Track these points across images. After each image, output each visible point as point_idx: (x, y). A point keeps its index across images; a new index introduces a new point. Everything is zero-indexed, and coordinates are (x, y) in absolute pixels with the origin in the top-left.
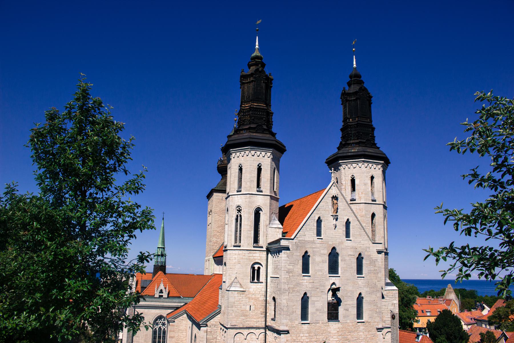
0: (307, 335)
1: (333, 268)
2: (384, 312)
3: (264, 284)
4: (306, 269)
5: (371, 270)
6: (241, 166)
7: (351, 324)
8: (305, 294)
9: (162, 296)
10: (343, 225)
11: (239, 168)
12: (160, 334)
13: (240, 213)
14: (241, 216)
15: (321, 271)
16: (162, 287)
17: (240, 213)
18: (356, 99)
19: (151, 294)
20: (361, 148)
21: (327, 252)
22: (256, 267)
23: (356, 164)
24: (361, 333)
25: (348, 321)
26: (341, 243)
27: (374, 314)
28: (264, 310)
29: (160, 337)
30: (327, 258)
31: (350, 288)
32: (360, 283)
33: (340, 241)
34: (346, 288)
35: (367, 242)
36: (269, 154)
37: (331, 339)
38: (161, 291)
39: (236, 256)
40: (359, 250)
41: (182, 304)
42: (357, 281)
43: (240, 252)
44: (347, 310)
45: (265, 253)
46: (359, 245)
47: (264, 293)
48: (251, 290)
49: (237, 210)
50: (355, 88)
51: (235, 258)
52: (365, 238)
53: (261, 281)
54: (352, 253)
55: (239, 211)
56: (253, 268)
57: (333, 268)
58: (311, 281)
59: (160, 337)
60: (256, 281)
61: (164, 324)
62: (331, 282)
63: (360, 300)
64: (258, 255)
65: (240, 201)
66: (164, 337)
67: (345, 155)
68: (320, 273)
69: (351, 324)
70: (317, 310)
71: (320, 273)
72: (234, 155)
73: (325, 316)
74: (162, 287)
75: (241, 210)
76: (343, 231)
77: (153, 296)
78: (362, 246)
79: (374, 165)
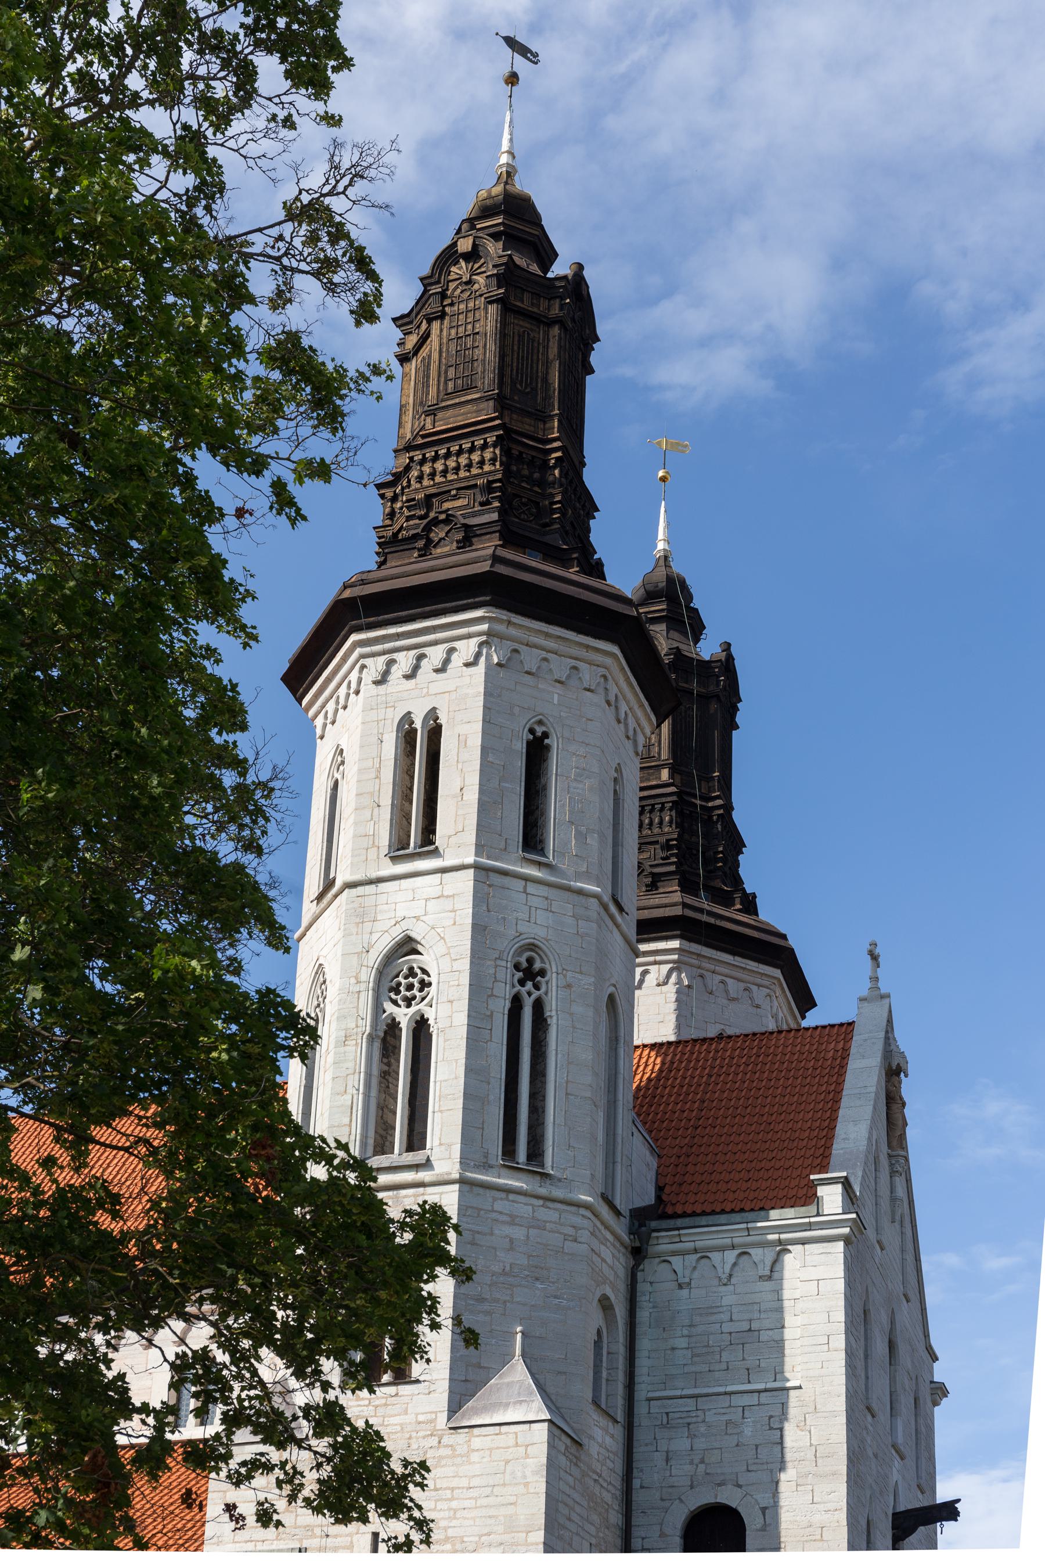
6: (539, 730)
11: (531, 737)
13: (537, 987)
14: (538, 1007)
17: (537, 987)
23: (742, 985)
39: (518, 1233)
43: (549, 1214)
49: (517, 967)
51: (511, 1241)
55: (530, 974)
65: (541, 917)
75: (542, 973)
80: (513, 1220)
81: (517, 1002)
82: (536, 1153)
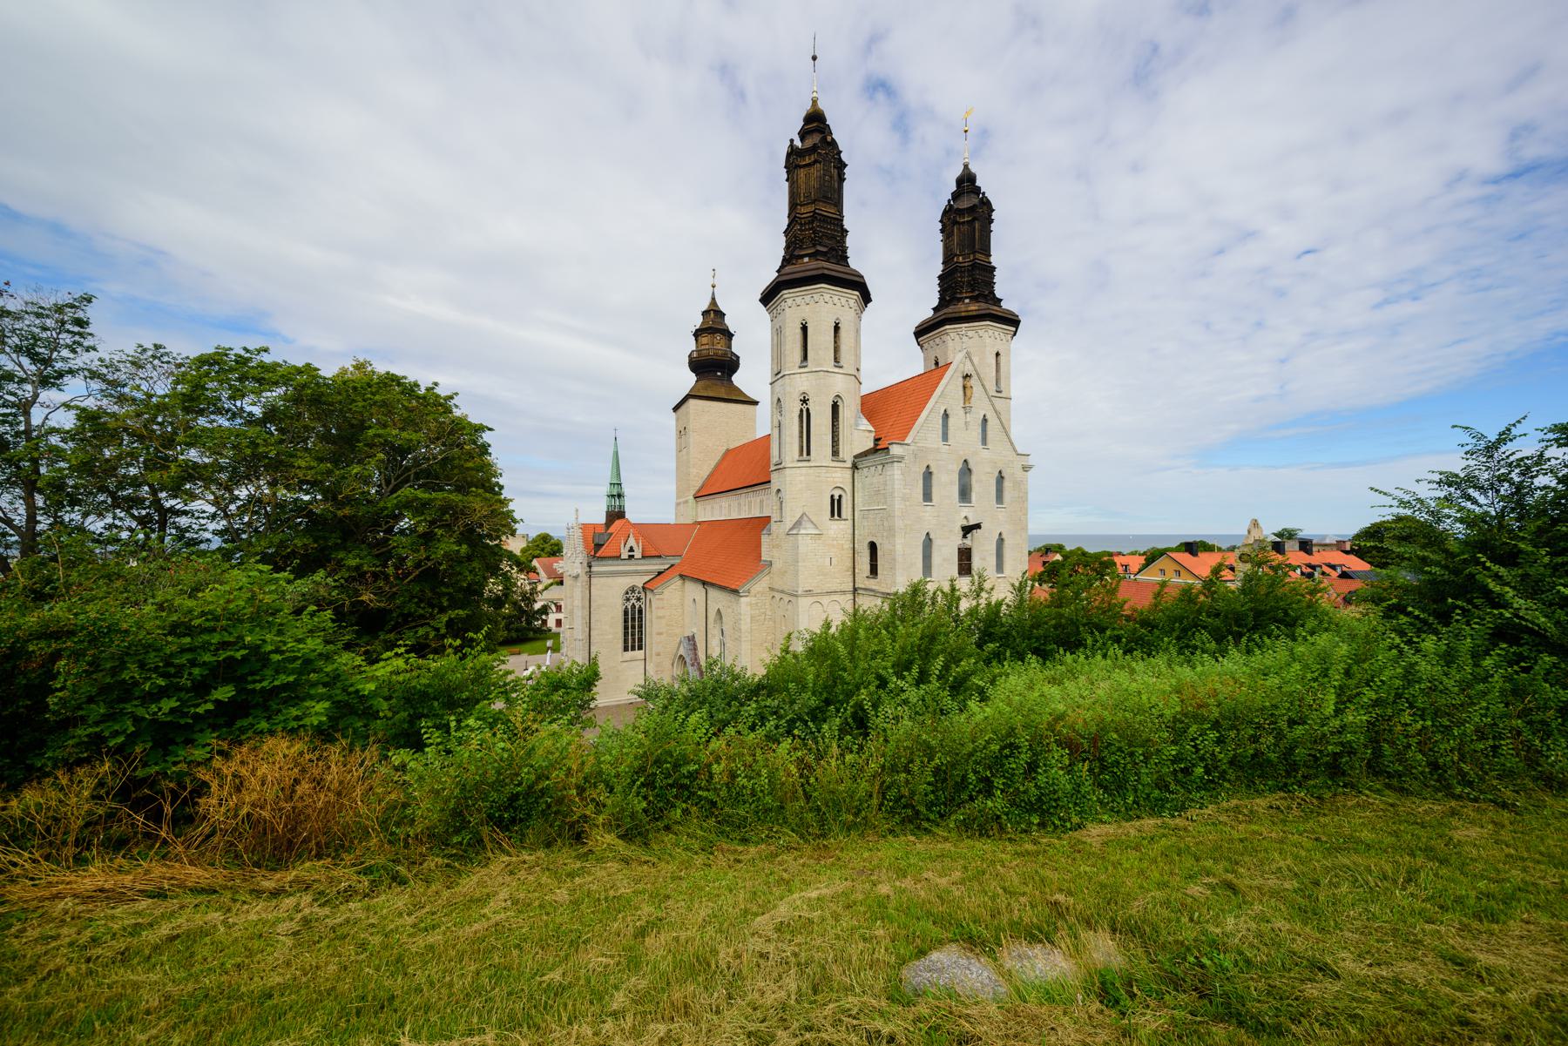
1: (965, 494)
3: (850, 522)
4: (927, 496)
9: (633, 556)
12: (633, 614)
14: (808, 410)
16: (632, 542)
18: (974, 219)
19: (615, 554)
20: (983, 305)
21: (958, 466)
22: (837, 494)
28: (851, 565)
29: (633, 619)
30: (956, 477)
36: (852, 302)
38: (631, 550)
39: (803, 478)
40: (1000, 466)
41: (666, 567)
44: (984, 559)
45: (849, 472)
47: (850, 537)
48: (832, 532)
50: (965, 204)
53: (844, 515)
54: (989, 470)
55: (805, 401)
56: (832, 496)
57: (965, 494)
58: (936, 514)
59: (633, 619)
60: (836, 517)
61: (639, 599)
63: (1001, 541)
64: (839, 475)
66: (640, 619)
67: (957, 315)
70: (944, 560)
72: (790, 302)
74: (632, 542)
77: (618, 557)
80: (801, 475)
81: (801, 411)
82: (808, 454)
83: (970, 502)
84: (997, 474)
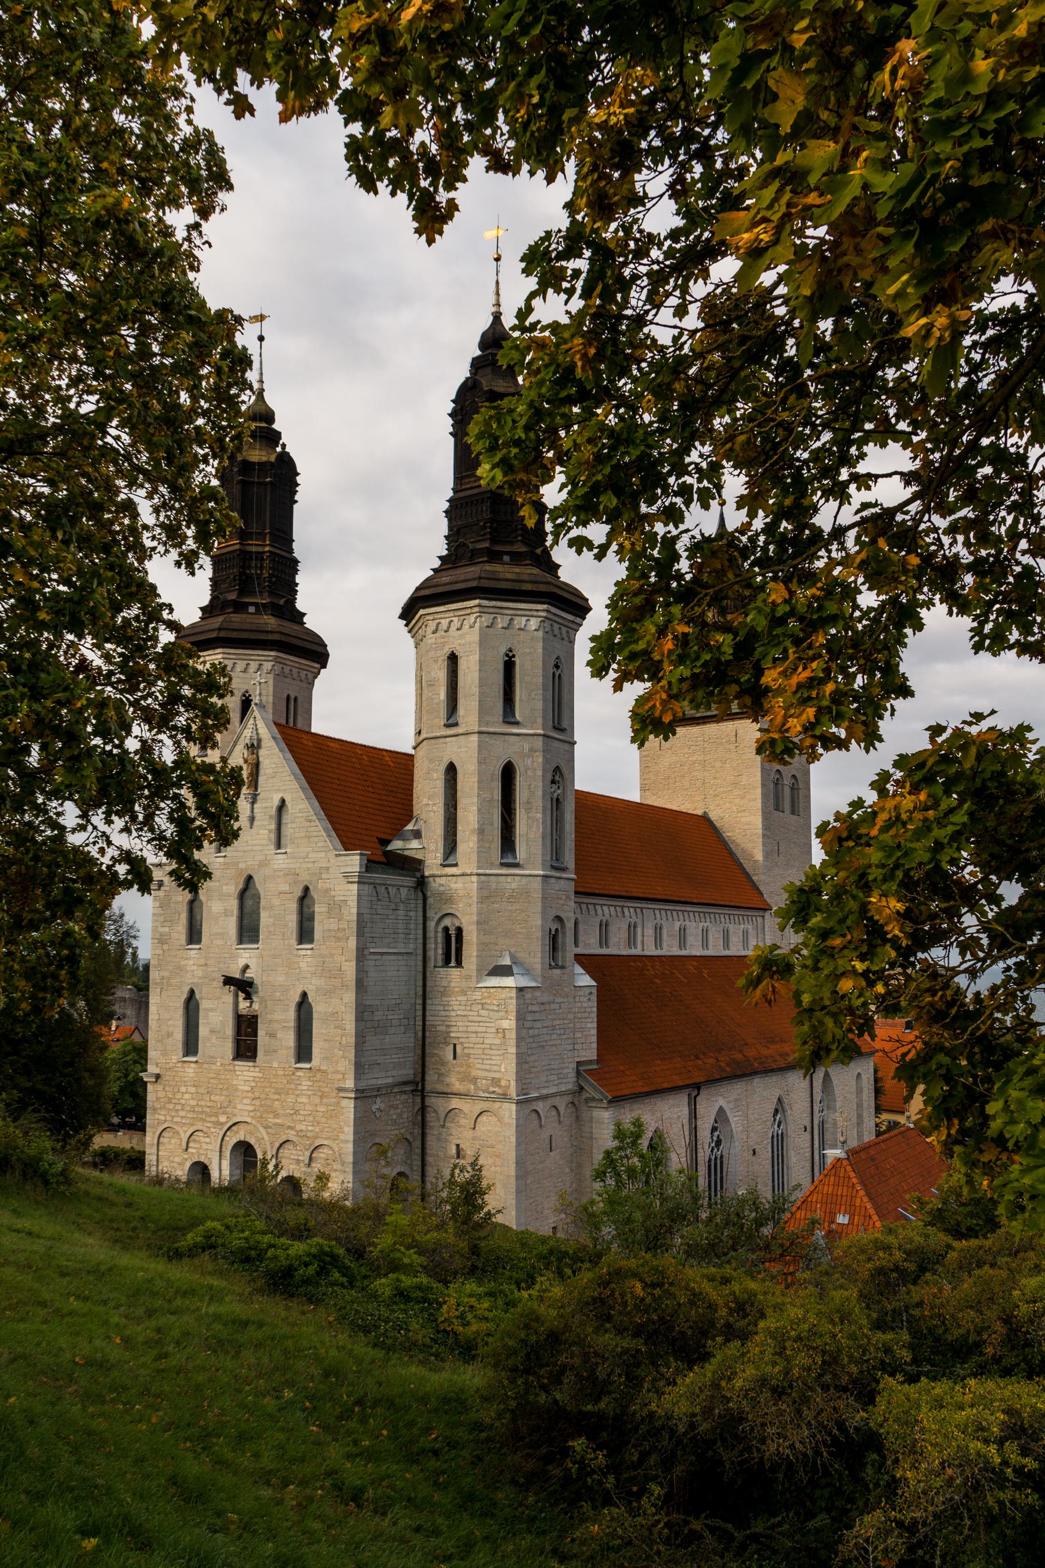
0: (193, 1090)
2: (471, 1051)
5: (329, 930)
7: (281, 1073)
8: (192, 992)
10: (271, 817)
15: (222, 935)
21: (232, 889)
24: (304, 1100)
25: (275, 1065)
26: (264, 864)
27: (336, 1051)
31: (280, 979)
32: (303, 965)
33: (263, 858)
34: (271, 979)
35: (323, 855)
37: (239, 1107)
40: (305, 878)
42: (297, 959)
44: (272, 1035)
46: (304, 866)
52: (320, 844)
54: (285, 888)
58: (202, 961)
62: (242, 963)
68: (219, 942)
69: (281, 1073)
71: (219, 942)
73: (228, 1048)
76: (270, 831)
78: (310, 865)
79: (455, 619)
83: (257, 941)
84: (299, 893)
